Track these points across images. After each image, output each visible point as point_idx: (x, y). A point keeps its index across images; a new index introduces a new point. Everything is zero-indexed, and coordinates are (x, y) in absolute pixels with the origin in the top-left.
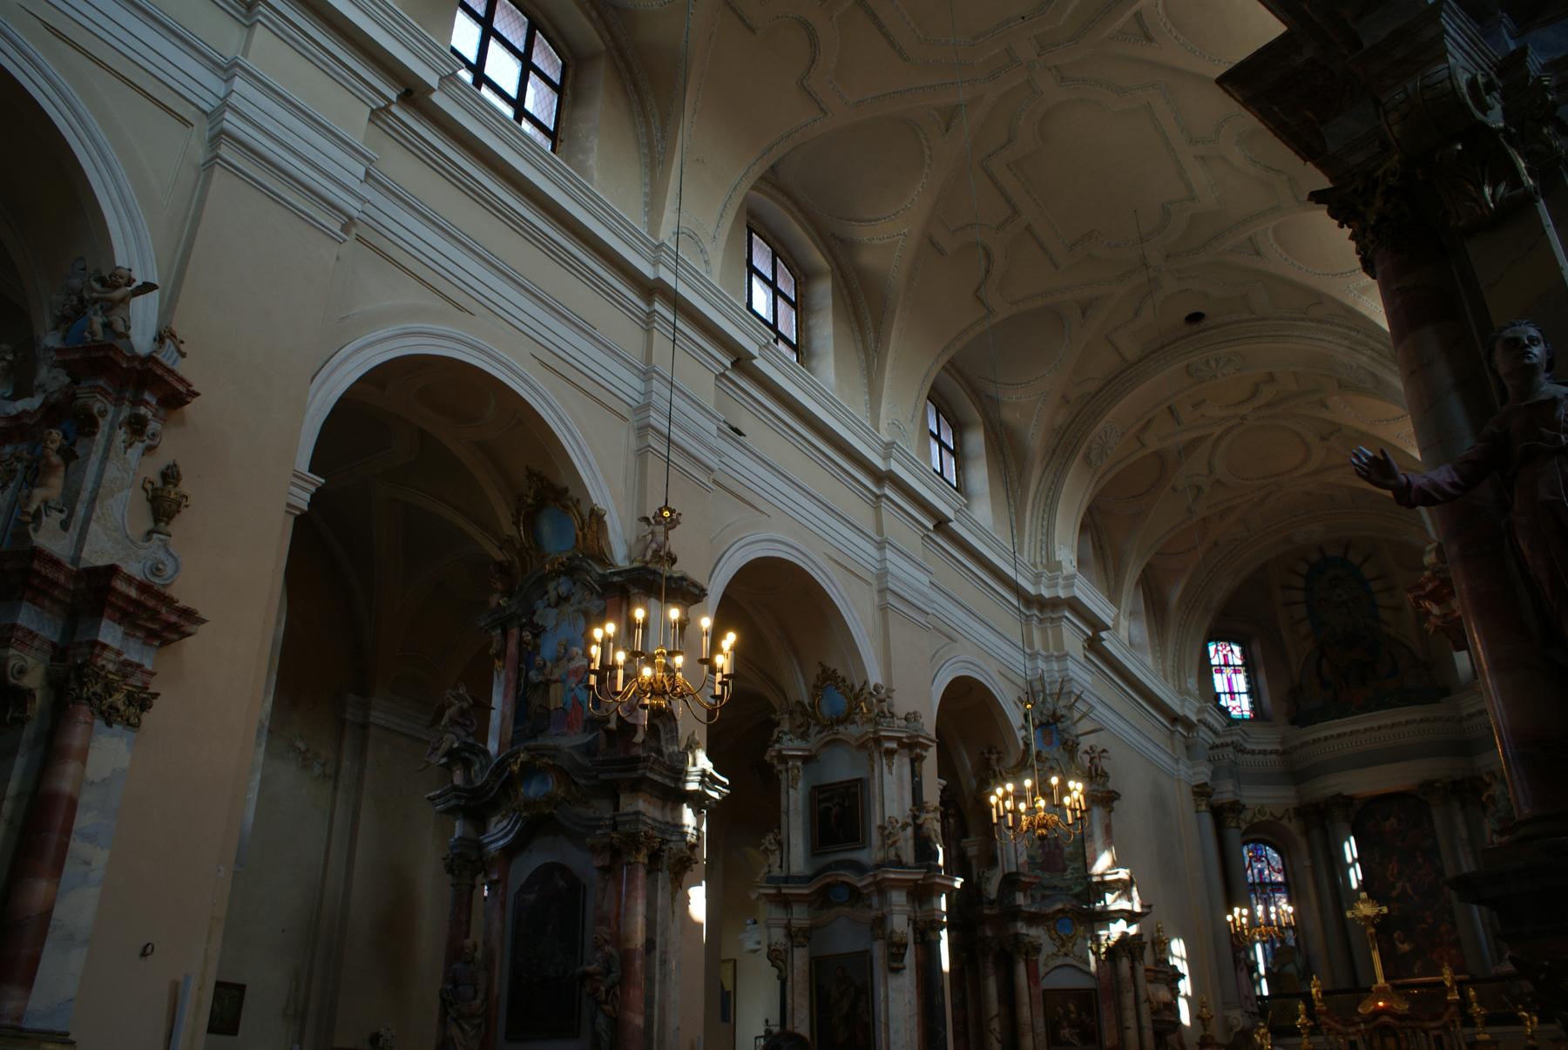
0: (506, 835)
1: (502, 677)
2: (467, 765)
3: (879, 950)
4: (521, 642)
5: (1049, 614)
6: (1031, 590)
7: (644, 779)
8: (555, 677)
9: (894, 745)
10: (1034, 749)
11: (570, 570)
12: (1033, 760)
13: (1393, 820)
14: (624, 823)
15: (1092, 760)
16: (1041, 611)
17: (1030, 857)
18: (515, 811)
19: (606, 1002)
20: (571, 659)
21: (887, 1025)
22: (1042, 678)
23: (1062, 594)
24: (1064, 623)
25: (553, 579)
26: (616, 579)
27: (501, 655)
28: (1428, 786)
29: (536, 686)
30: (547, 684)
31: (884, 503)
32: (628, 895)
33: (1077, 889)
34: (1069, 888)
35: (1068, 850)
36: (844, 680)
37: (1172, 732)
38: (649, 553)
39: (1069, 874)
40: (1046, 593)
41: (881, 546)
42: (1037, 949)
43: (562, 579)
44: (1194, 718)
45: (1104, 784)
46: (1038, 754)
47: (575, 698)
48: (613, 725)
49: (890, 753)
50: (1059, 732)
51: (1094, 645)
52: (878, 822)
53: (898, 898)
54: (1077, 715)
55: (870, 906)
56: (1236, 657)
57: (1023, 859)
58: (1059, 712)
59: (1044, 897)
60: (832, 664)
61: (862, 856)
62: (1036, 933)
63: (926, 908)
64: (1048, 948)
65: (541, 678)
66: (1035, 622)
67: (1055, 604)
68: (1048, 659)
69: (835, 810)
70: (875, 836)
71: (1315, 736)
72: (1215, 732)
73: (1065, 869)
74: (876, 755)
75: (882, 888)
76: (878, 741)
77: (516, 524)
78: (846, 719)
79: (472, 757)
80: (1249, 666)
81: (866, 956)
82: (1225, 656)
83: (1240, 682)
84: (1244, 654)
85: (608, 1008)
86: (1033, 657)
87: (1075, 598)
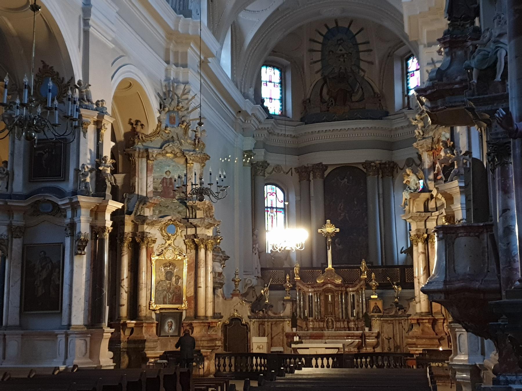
3: (68, 241)
13: (346, 180)
17: (155, 189)
28: (367, 164)
36: (58, 74)
51: (203, 64)
55: (65, 216)
57: (150, 189)
61: (62, 186)
64: (160, 241)
69: (46, 156)
71: (313, 130)
80: (283, 83)
83: (276, 93)
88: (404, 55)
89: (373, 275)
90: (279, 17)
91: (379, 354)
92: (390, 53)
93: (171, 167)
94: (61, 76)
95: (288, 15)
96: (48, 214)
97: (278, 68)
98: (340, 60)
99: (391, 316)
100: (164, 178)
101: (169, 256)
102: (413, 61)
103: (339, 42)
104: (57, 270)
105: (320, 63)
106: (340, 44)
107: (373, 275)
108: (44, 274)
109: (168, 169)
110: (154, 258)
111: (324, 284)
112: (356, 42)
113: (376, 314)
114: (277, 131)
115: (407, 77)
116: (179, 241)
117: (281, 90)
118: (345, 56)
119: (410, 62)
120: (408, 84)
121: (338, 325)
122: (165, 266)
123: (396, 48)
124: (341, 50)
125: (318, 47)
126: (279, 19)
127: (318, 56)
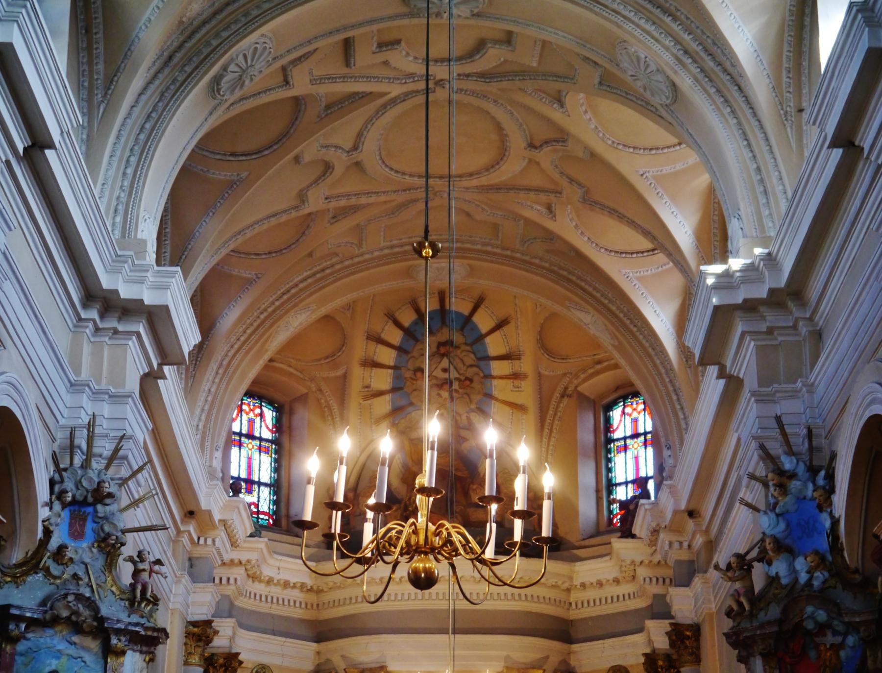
5: (112, 323)
6: (106, 282)
10: (54, 544)
12: (47, 561)
15: (136, 573)
16: (102, 316)
22: (91, 426)
23: (149, 298)
37: (179, 532)
40: (126, 292)
44: (217, 516)
45: (150, 615)
46: (59, 554)
50: (97, 519)
54: (125, 501)
66: (89, 329)
67: (130, 310)
68: (97, 395)
72: (234, 544)
82: (251, 422)
84: (278, 427)
86: (75, 387)
87: (166, 308)
88: (602, 396)
90: (306, 274)
92: (566, 388)
93: (64, 659)
95: (328, 271)
97: (271, 403)
98: (439, 395)
102: (623, 413)
103: (442, 350)
105: (388, 397)
106: (443, 355)
112: (486, 351)
114: (267, 572)
115: (609, 451)
117: (276, 461)
118: (456, 386)
119: (616, 414)
120: (609, 470)
123: (583, 376)
124: (445, 370)
125: (387, 356)
126: (305, 279)
127: (382, 380)
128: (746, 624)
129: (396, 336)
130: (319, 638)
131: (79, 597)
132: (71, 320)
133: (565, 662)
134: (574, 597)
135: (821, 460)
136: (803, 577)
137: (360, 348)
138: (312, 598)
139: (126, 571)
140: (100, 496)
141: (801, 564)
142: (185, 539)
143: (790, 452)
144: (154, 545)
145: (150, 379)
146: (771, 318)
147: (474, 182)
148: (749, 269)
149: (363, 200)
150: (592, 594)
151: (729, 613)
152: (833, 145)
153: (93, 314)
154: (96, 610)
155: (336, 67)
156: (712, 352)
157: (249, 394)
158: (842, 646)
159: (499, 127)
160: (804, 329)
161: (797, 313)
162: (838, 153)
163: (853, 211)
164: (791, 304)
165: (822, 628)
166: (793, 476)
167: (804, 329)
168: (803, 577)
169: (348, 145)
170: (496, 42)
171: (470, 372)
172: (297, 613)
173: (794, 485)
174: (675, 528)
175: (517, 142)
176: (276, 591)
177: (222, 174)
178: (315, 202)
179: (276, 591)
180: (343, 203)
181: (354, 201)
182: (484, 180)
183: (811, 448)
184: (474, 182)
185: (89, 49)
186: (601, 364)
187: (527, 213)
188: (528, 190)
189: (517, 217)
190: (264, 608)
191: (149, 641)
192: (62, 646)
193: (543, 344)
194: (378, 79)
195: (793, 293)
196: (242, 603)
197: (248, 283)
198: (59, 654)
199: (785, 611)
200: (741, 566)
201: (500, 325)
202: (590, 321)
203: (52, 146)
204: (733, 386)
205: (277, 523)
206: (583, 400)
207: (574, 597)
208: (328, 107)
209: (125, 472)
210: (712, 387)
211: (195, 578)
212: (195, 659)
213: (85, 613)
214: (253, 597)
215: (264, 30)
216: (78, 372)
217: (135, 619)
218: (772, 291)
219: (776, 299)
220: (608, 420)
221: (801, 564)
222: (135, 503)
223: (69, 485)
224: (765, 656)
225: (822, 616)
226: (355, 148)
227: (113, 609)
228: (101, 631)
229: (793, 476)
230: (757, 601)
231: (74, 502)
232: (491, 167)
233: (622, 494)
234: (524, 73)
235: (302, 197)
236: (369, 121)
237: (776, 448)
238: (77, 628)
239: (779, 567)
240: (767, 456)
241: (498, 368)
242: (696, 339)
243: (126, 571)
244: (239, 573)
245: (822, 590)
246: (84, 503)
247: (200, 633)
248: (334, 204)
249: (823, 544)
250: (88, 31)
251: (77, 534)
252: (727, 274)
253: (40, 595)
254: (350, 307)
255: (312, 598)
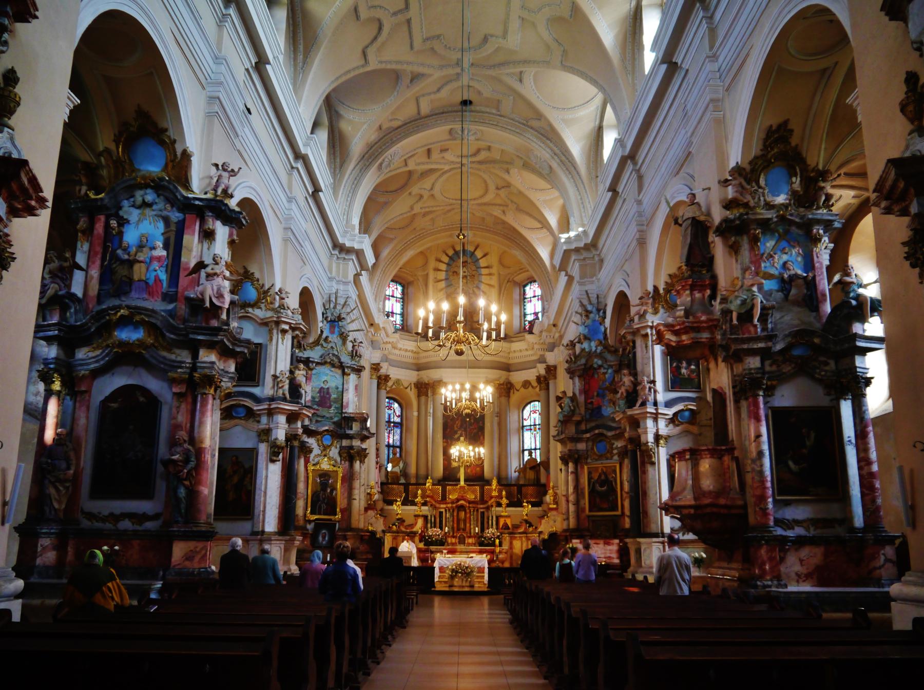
0: (96, 362)
1: (86, 247)
2: (64, 309)
3: (263, 448)
4: (107, 226)
5: (343, 255)
6: (341, 240)
7: (222, 341)
8: (141, 259)
9: (286, 327)
10: (324, 336)
11: (157, 185)
12: (322, 342)
14: (201, 367)
15: (353, 346)
17: (313, 398)
18: (108, 346)
19: (185, 480)
20: (154, 248)
21: (265, 493)
22: (336, 293)
23: (356, 246)
24: (351, 263)
25: (141, 189)
26: (197, 203)
27: (89, 232)
29: (123, 262)
30: (131, 263)
31: (295, 173)
32: (203, 413)
33: (336, 419)
34: (331, 418)
35: (334, 396)
36: (258, 280)
38: (219, 191)
39: (332, 410)
40: (348, 244)
41: (290, 200)
42: (311, 451)
43: (149, 191)
44: (381, 326)
46: (326, 339)
47: (157, 277)
48: (208, 304)
49: (284, 332)
50: (339, 327)
52: (272, 373)
53: (282, 419)
54: (349, 321)
55: (259, 422)
56: (398, 293)
58: (343, 316)
59: (317, 421)
60: (254, 269)
61: (256, 391)
62: (312, 442)
63: (293, 426)
64: (316, 451)
65: (126, 257)
67: (349, 251)
68: (338, 282)
70: (269, 380)
72: (387, 336)
73: (330, 407)
74: (275, 331)
75: (271, 413)
76: (278, 323)
77: (117, 141)
78: (255, 305)
79: (71, 304)
81: (252, 453)
83: (398, 308)
84: (403, 293)
85: (187, 483)
86: (330, 279)
89: (504, 493)
91: (507, 569)
94: (261, 282)
96: (240, 418)
97: (400, 284)
99: (520, 533)
100: (322, 388)
101: (325, 465)
104: (249, 476)
107: (504, 493)
108: (236, 479)
109: (325, 378)
110: (311, 468)
111: (458, 500)
113: (506, 531)
114: (400, 346)
116: (334, 452)
119: (527, 288)
121: (470, 541)
122: (321, 476)
127: (442, 275)
128: (573, 366)
129: (446, 259)
130: (418, 370)
131: (334, 355)
132: (328, 254)
133: (507, 379)
134: (511, 355)
135: (601, 307)
136: (594, 349)
137: (432, 264)
138: (415, 355)
139: (349, 346)
140: (340, 318)
141: (593, 344)
142: (370, 334)
143: (590, 303)
144: (359, 336)
145: (357, 276)
146: (585, 254)
147: (476, 202)
148: (577, 236)
149: (435, 209)
150: (517, 354)
151: (567, 362)
152: (609, 191)
153: (336, 252)
154: (339, 359)
155: (425, 159)
156: (563, 267)
157: (392, 281)
158: (606, 373)
159: (485, 182)
160: (597, 258)
161: (594, 252)
162: (610, 194)
163: (615, 216)
164: (592, 249)
165: (600, 367)
166: (591, 312)
167: (597, 258)
168: (594, 349)
169: (429, 188)
170: (484, 149)
171: (474, 273)
172: (411, 361)
173: (592, 316)
174: (549, 330)
175: (492, 187)
176: (403, 353)
177: (382, 199)
178: (417, 209)
179: (403, 353)
180: (427, 210)
181: (431, 209)
182: (479, 201)
183: (598, 303)
184: (476, 202)
185: (334, 154)
186: (522, 270)
187: (495, 213)
188: (496, 205)
189: (492, 215)
190: (399, 359)
191: (358, 370)
192: (328, 372)
193: (501, 262)
194: (440, 163)
195: (593, 245)
196: (391, 357)
197: (392, 240)
198: (327, 375)
199: (587, 361)
200: (572, 345)
201: (485, 255)
202: (518, 254)
203: (321, 191)
204: (571, 279)
205: (403, 328)
206: (516, 283)
207: (511, 355)
208: (422, 174)
209: (349, 310)
210: (563, 279)
211: (374, 348)
212: (374, 377)
213: (336, 360)
214: (395, 355)
215: (398, 145)
216: (331, 273)
217: (353, 362)
218: (585, 244)
219: (587, 247)
220: (524, 291)
221: (593, 344)
222: (353, 321)
223: (329, 315)
224: (579, 377)
225: (600, 362)
226: (432, 189)
227: (346, 359)
228: (342, 367)
229: (591, 312)
230: (576, 357)
231: (331, 321)
232: (482, 197)
233: (530, 318)
234: (494, 162)
235: (412, 208)
236: (437, 179)
237: (585, 302)
238: (333, 366)
239: (585, 345)
240: (582, 305)
241: (484, 271)
242: (557, 262)
243: (349, 346)
244: (389, 346)
245: (600, 353)
246: (334, 321)
247: (376, 367)
248: (423, 210)
249: (601, 337)
250: (334, 147)
251: (332, 332)
252: (569, 238)
253: (320, 354)
254: (428, 248)
255: (415, 355)
